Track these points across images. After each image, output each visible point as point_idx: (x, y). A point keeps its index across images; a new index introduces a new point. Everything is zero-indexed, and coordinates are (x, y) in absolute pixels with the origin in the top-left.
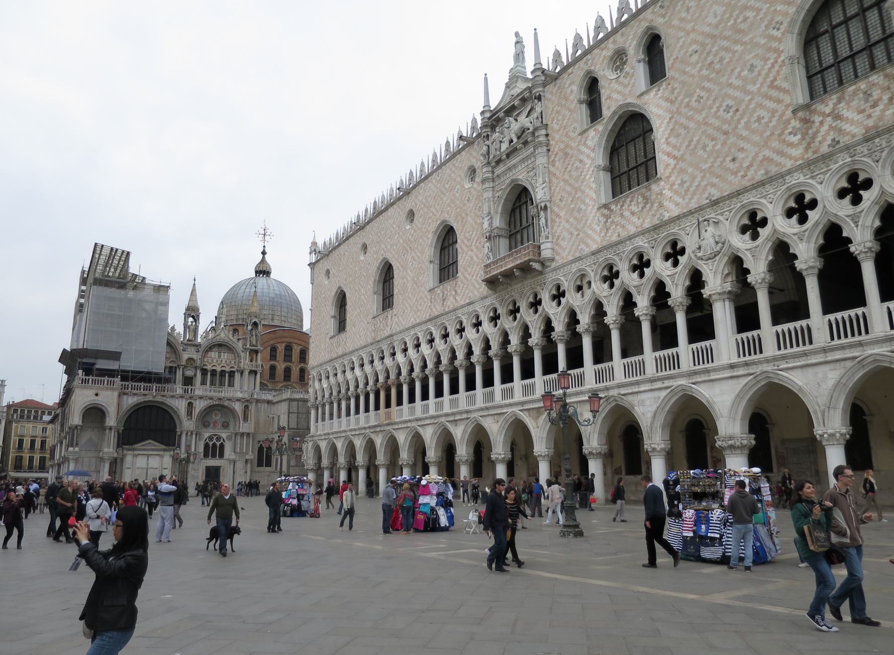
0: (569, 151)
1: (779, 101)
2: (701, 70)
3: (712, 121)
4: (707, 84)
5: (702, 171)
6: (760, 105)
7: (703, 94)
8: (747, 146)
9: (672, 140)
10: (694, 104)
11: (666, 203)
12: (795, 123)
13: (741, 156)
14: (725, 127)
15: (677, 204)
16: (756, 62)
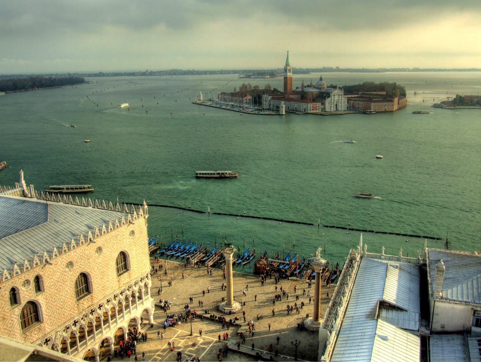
0: (5, 317)
1: (73, 300)
2: (55, 290)
3: (58, 305)
4: (56, 295)
5: (57, 318)
6: (69, 301)
7: (56, 297)
8: (66, 311)
9: (47, 311)
10: (53, 300)
11: (47, 329)
12: (76, 305)
13: (65, 314)
14: (62, 307)
15: (50, 329)
16: (68, 290)
